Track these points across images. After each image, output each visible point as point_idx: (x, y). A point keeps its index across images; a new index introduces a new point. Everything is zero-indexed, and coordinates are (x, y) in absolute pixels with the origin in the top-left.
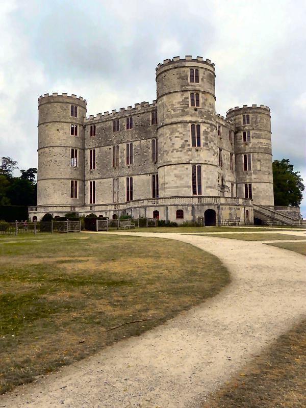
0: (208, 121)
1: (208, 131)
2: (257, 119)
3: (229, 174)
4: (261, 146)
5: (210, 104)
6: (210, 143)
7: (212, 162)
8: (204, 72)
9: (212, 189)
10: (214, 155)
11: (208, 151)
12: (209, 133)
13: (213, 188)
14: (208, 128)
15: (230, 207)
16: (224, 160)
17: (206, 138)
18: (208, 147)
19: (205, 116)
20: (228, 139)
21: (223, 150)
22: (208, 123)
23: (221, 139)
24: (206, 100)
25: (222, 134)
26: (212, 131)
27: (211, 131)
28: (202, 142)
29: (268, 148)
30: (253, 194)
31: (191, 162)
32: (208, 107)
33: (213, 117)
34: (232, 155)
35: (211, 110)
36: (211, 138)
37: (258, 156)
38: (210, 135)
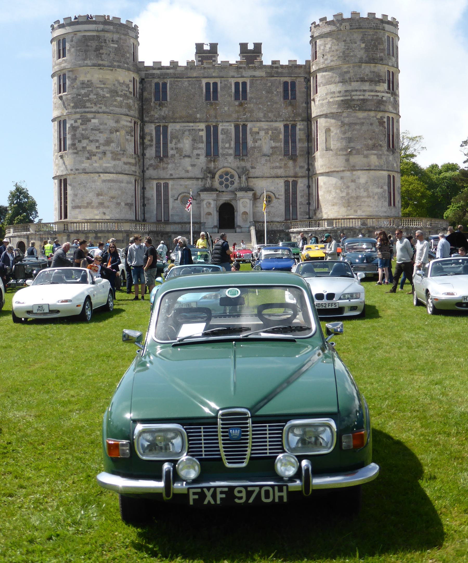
0: (78, 110)
1: (76, 125)
2: (325, 47)
3: (278, 164)
4: (331, 100)
5: (83, 83)
6: (80, 141)
7: (84, 169)
8: (73, 37)
9: (83, 210)
10: (88, 159)
11: (75, 155)
12: (78, 127)
13: (87, 207)
14: (76, 122)
15: (41, 237)
16: (255, 141)
17: (74, 137)
18: (76, 149)
19: (72, 105)
20: (279, 99)
21: (249, 125)
22: (76, 113)
23: (241, 105)
24: (75, 79)
25: (249, 96)
26: (86, 121)
27: (81, 124)
28: (68, 142)
29: (354, 100)
30: (320, 198)
31: (58, 174)
32: (78, 89)
33: (89, 101)
34: (294, 126)
35: (83, 92)
36: (82, 135)
37: (326, 122)
38: (80, 131)
